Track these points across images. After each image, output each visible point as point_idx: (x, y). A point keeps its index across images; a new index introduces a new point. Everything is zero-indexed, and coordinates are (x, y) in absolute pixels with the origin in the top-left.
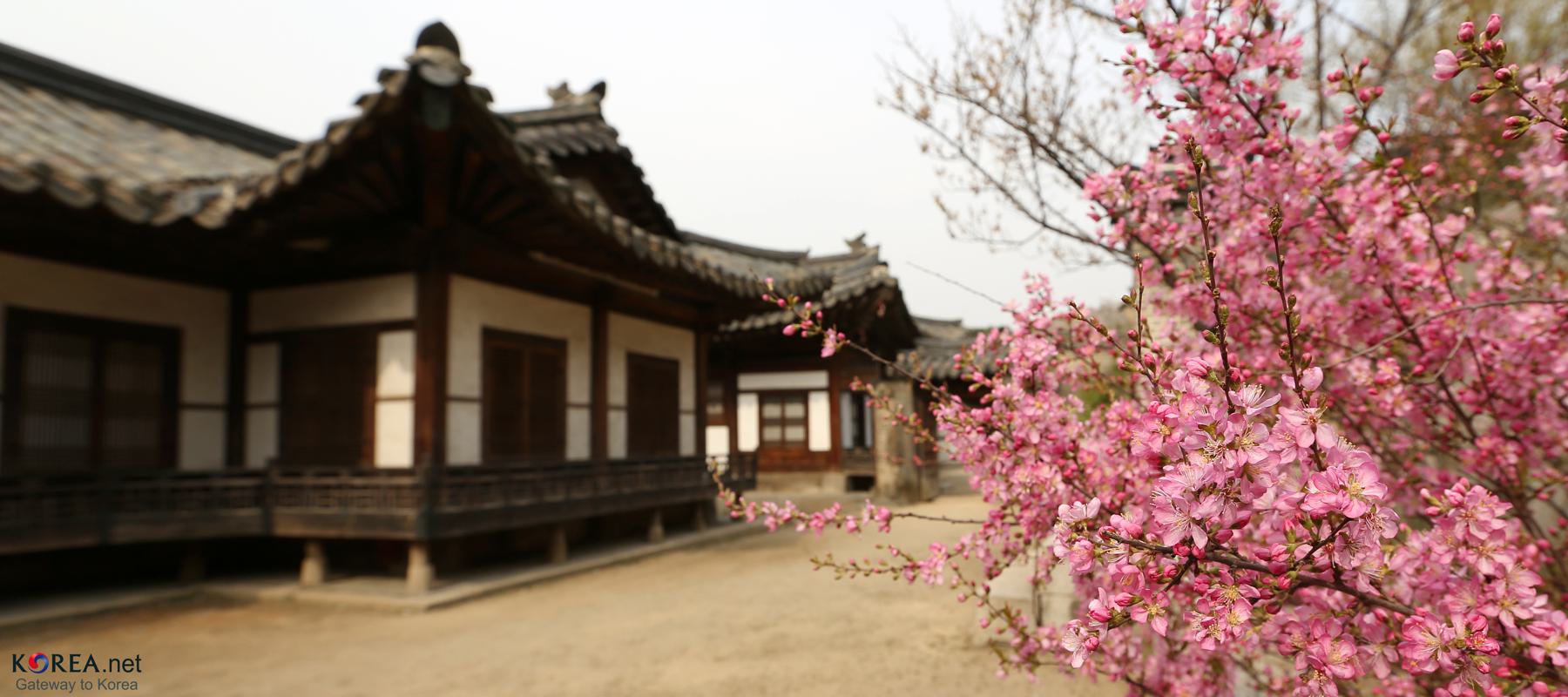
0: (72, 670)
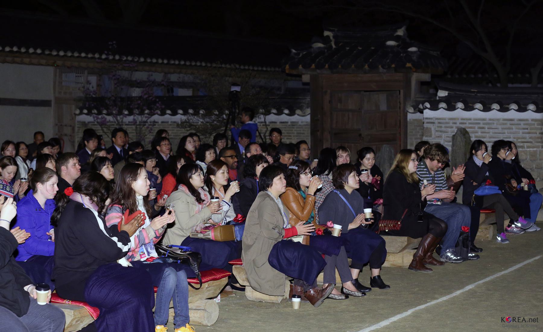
0: (518, 322)
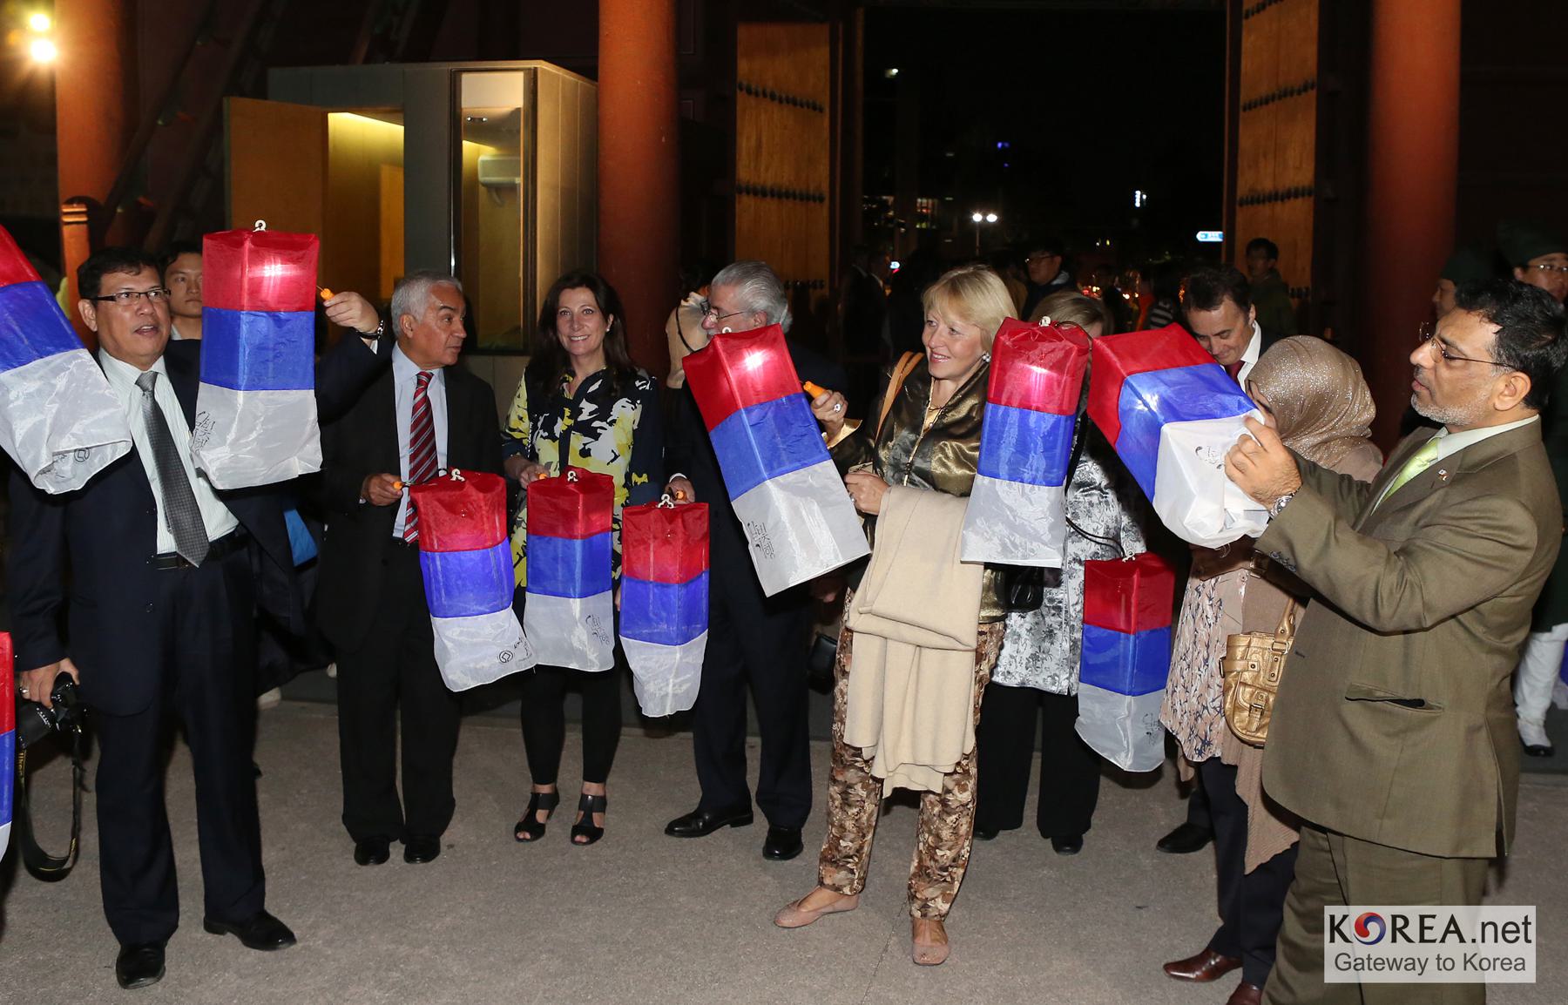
0: (1422, 940)
